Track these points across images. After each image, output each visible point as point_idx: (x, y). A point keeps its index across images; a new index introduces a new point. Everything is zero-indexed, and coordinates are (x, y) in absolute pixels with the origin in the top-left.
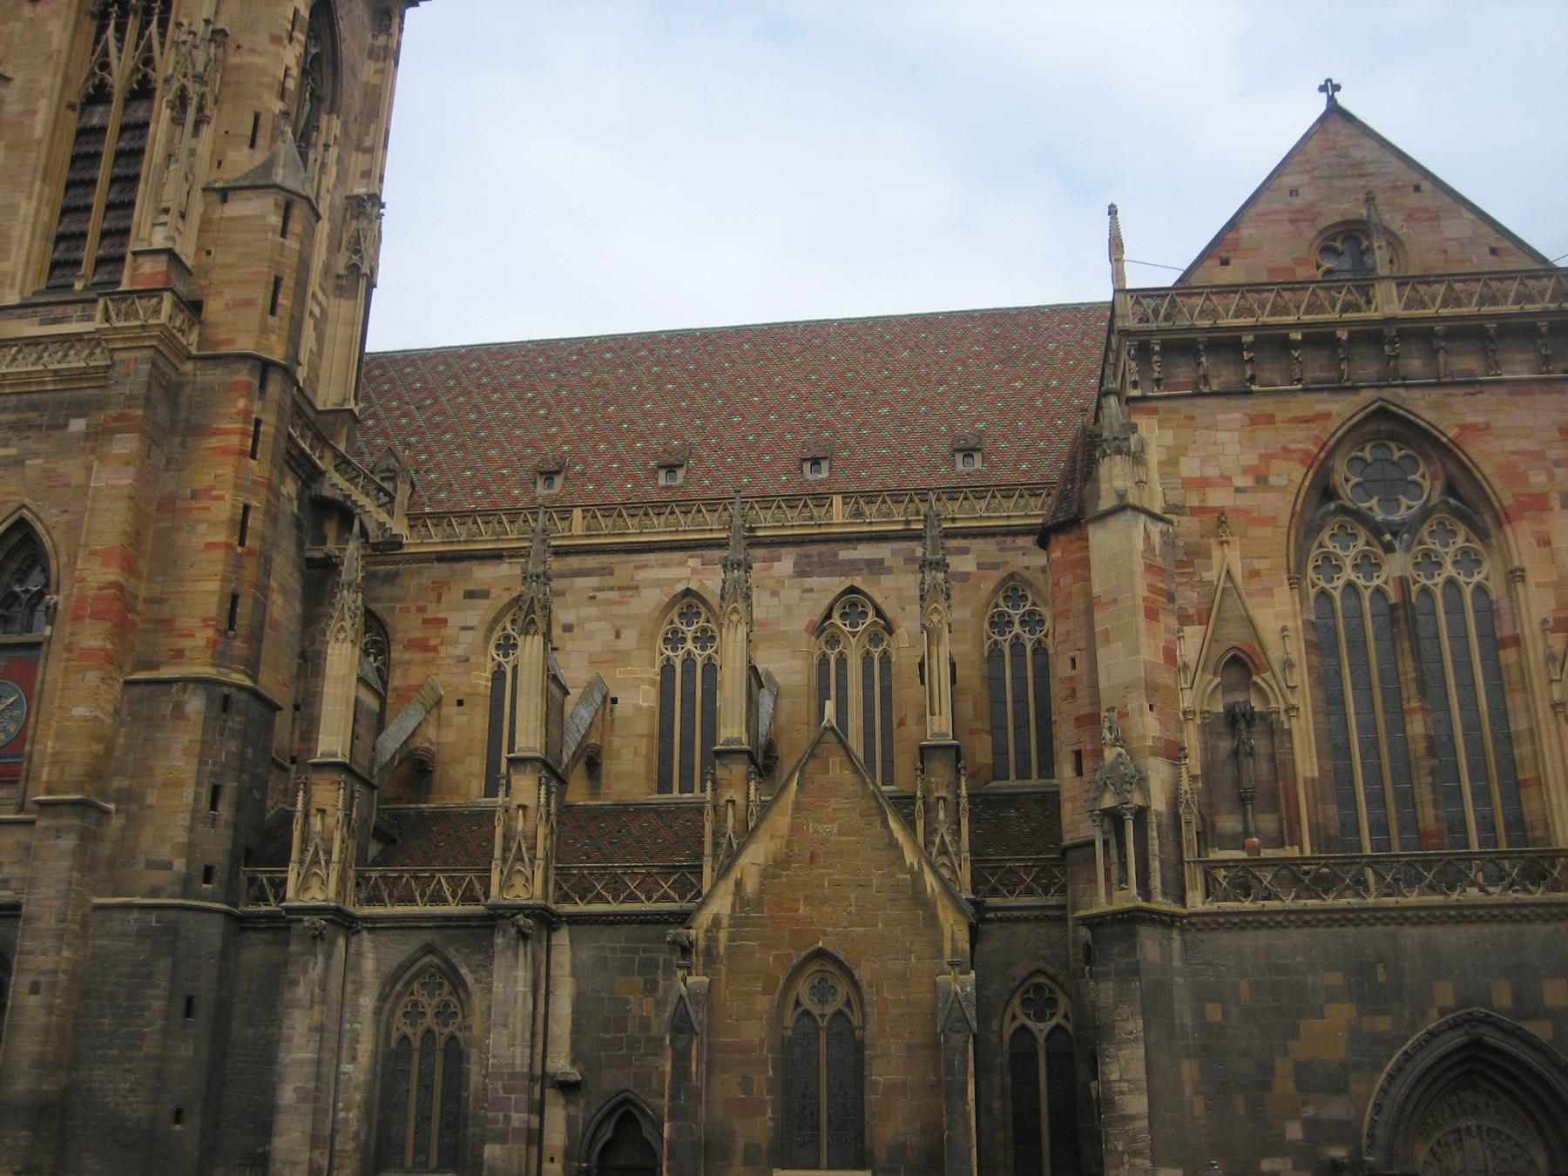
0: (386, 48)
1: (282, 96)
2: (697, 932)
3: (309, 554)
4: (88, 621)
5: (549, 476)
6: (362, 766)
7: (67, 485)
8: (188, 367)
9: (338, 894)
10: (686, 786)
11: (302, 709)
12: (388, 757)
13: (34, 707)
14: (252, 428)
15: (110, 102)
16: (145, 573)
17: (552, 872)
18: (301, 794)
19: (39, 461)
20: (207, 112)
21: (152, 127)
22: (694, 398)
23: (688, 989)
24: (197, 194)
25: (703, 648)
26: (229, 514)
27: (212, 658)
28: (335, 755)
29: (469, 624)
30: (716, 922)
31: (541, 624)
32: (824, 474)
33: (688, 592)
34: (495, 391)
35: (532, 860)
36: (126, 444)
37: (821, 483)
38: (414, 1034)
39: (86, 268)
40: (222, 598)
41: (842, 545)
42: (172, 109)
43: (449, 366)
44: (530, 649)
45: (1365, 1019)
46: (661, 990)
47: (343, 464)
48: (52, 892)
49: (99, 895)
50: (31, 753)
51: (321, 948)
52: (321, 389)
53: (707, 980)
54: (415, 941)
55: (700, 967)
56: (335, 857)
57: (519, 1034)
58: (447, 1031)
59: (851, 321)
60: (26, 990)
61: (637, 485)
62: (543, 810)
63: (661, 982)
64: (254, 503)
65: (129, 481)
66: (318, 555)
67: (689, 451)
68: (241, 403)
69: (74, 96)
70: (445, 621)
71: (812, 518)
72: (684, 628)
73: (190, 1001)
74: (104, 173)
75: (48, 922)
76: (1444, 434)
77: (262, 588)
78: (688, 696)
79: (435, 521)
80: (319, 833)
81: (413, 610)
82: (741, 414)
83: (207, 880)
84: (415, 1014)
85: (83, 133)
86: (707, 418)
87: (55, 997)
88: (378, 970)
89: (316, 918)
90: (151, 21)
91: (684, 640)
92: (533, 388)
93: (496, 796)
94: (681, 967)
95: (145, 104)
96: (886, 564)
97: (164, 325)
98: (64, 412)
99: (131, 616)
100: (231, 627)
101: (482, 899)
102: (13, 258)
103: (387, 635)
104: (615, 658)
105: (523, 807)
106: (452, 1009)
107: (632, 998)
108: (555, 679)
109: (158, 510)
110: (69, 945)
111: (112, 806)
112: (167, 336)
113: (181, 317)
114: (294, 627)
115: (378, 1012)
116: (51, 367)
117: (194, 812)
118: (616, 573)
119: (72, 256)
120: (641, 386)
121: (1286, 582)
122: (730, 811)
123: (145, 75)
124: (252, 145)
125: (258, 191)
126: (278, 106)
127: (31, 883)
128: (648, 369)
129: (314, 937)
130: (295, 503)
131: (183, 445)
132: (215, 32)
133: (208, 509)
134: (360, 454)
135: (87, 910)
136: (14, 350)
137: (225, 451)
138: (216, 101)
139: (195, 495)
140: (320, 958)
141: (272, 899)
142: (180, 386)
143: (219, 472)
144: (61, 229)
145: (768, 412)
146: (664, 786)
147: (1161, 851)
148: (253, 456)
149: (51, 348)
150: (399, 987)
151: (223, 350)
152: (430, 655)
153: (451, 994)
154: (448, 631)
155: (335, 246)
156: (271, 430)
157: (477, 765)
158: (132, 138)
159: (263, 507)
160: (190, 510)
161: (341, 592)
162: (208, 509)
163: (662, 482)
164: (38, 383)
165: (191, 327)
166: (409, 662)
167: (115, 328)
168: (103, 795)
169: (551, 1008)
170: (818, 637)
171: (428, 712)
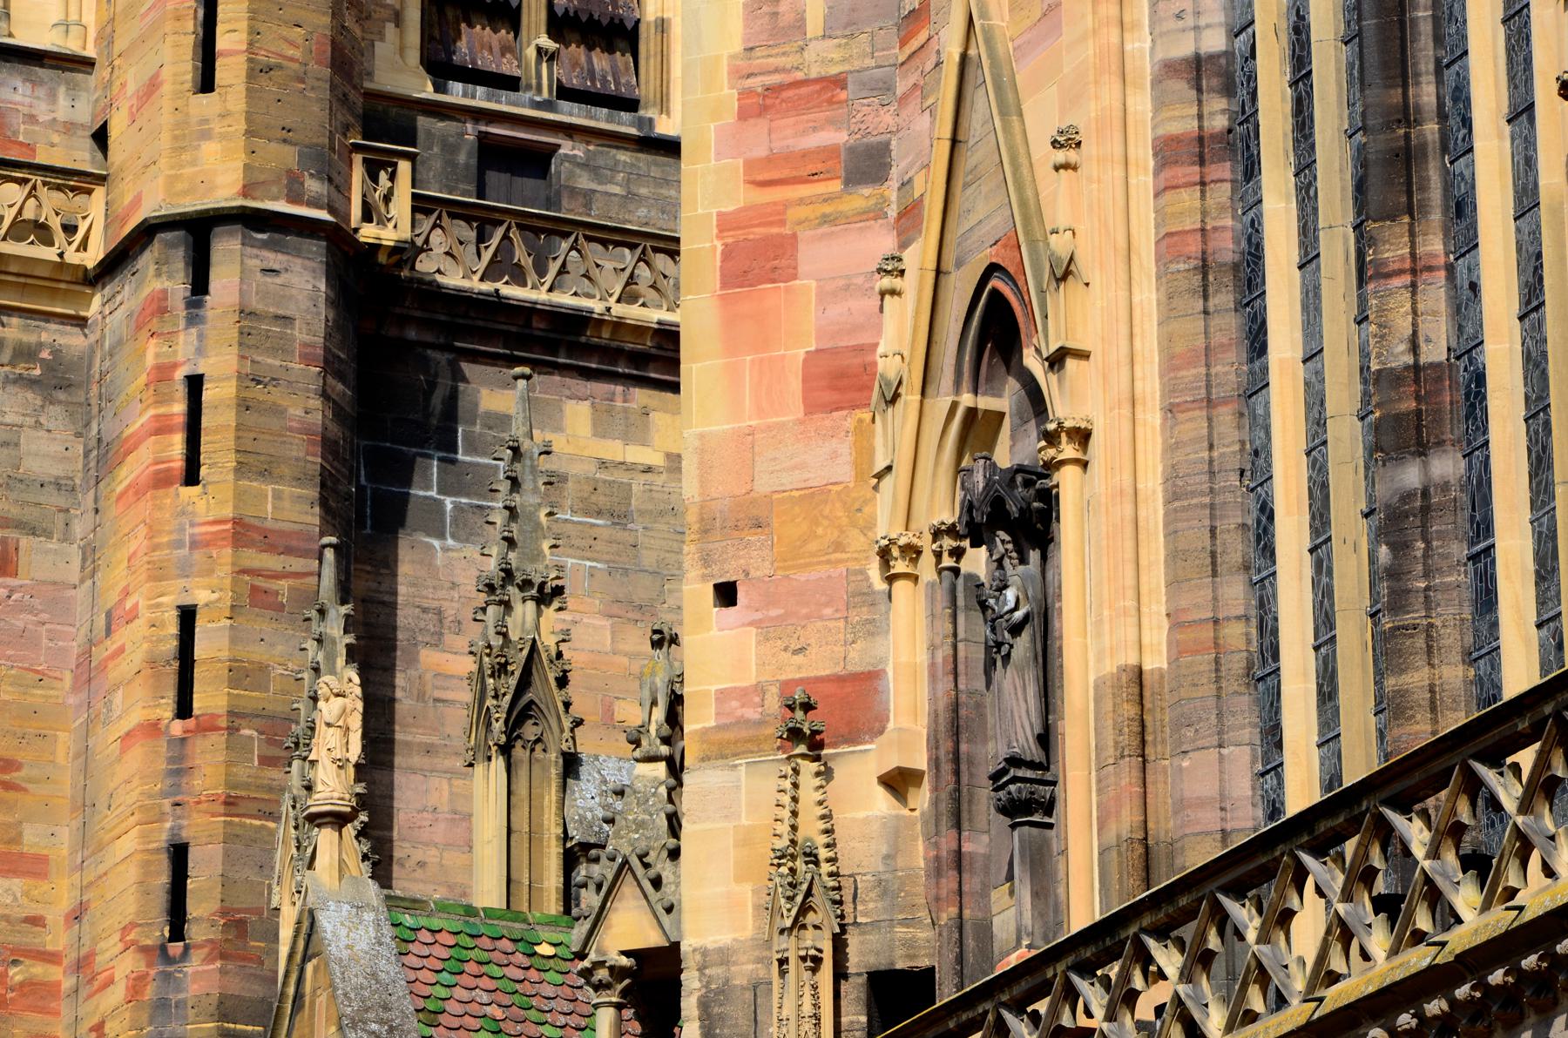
14: (179, 408)
64: (201, 596)
99: (16, 974)
100: (177, 933)
137: (137, 491)
148: (191, 476)
162: (121, 650)
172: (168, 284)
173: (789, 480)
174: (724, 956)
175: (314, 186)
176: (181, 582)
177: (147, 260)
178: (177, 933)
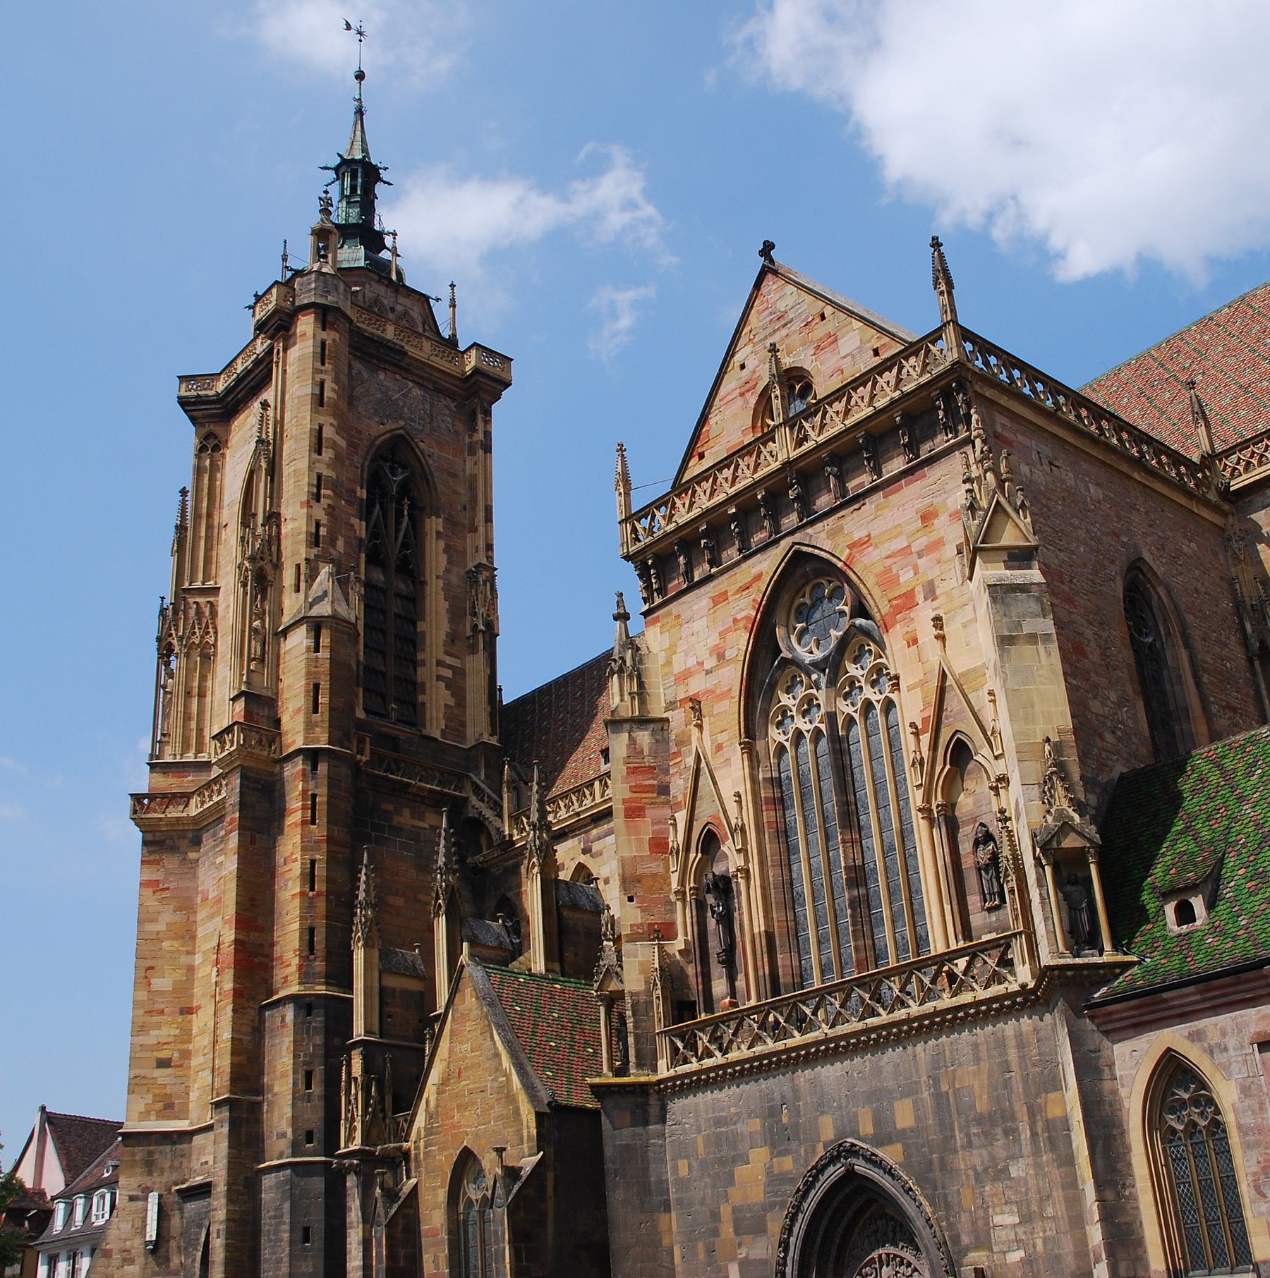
40: (301, 933)
45: (775, 1160)
64: (318, 857)
76: (840, 560)
99: (256, 960)
100: (311, 949)
117: (294, 1093)
121: (739, 748)
124: (298, 591)
147: (635, 1027)
148: (313, 822)
151: (291, 750)
156: (325, 799)
173: (648, 871)
174: (637, 994)
175: (346, 743)
177: (299, 759)
178: (311, 949)
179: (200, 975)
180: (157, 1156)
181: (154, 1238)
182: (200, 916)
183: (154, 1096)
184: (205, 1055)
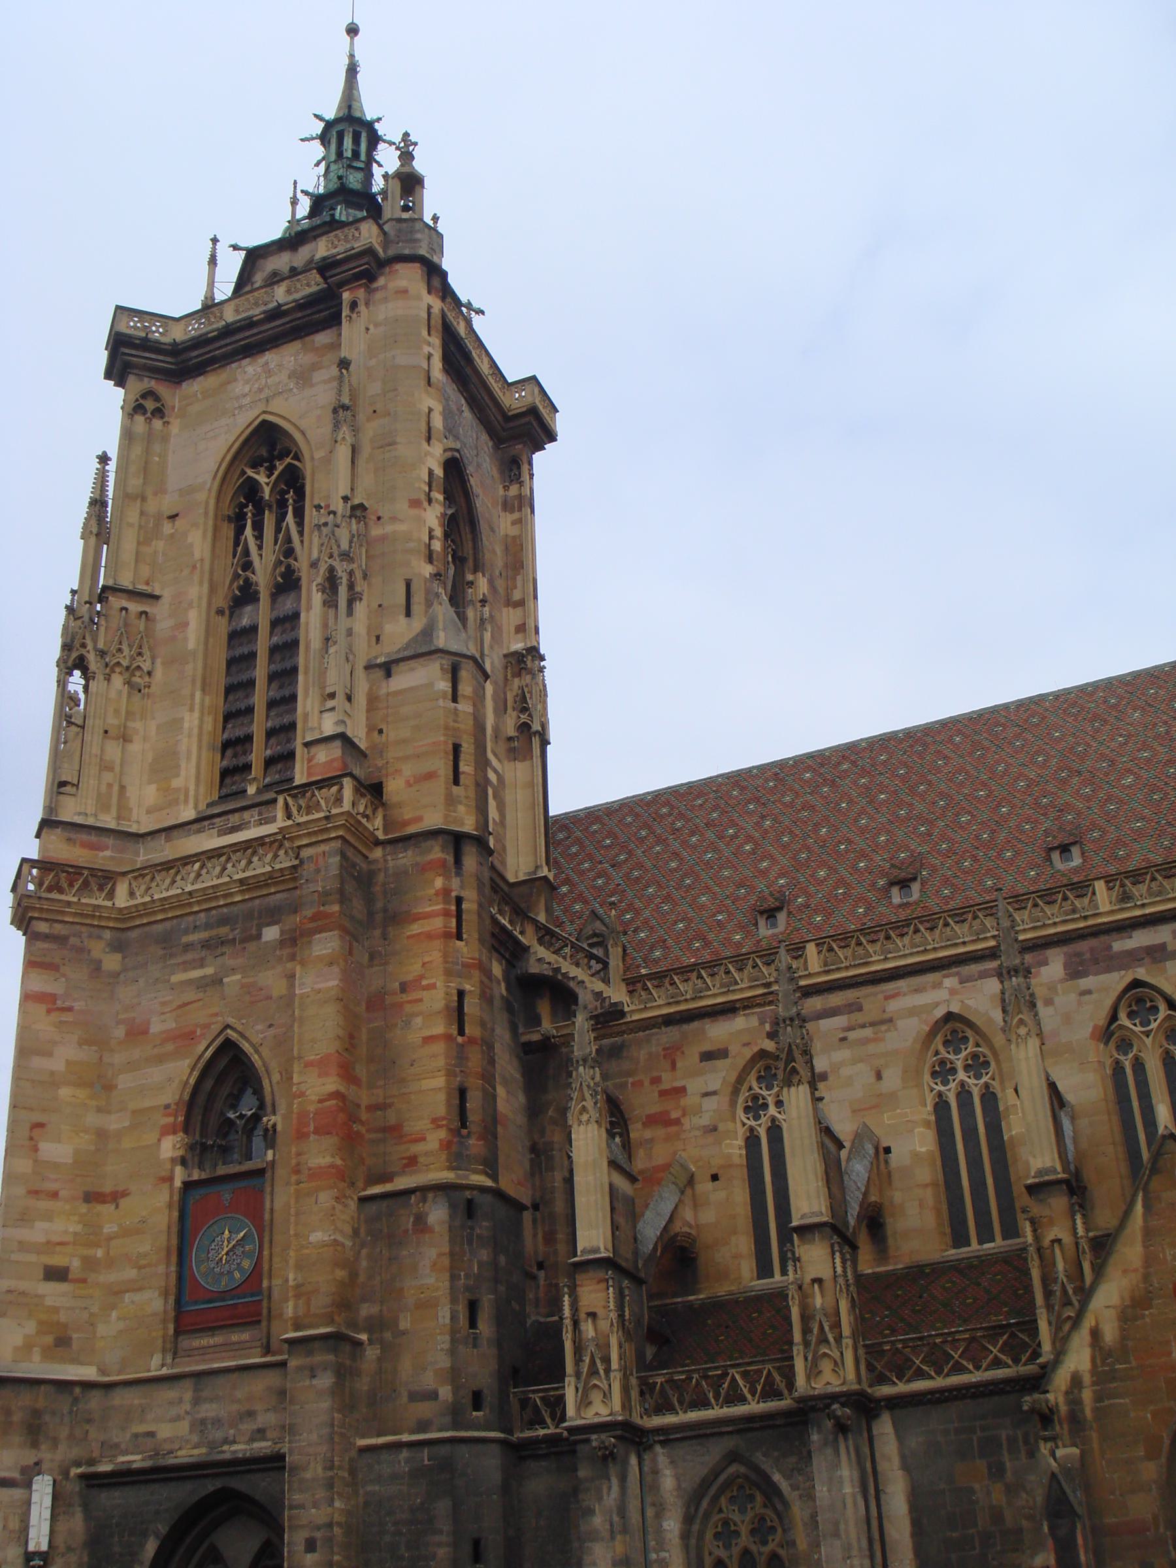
0: (520, 497)
1: (430, 559)
2: (1056, 1394)
3: (524, 1039)
4: (312, 1137)
5: (770, 914)
6: (627, 1260)
7: (269, 998)
8: (378, 853)
9: (623, 1407)
10: (986, 1235)
11: (541, 1207)
12: (651, 1247)
13: (266, 1239)
14: (453, 908)
15: (258, 600)
16: (364, 1079)
17: (861, 1351)
18: (566, 1298)
19: (238, 977)
20: (358, 589)
21: (303, 615)
22: (911, 805)
23: (1059, 1464)
24: (360, 673)
25: (978, 1076)
26: (444, 1002)
27: (448, 1160)
28: (597, 1250)
29: (711, 1089)
30: (1076, 1381)
31: (804, 1073)
32: (1077, 861)
33: (949, 1017)
34: (693, 834)
35: (839, 1338)
36: (326, 944)
37: (1076, 870)
38: (731, 1557)
39: (257, 770)
40: (449, 1094)
41: (1114, 935)
42: (323, 592)
43: (637, 815)
44: (798, 1098)
46: (1009, 1474)
47: (547, 936)
48: (314, 1437)
49: (363, 1437)
50: (270, 1288)
51: (613, 1471)
52: (510, 860)
53: (1075, 1451)
54: (715, 1451)
55: (1066, 1437)
56: (615, 1365)
57: (855, 1544)
58: (766, 1549)
59: (1067, 692)
60: (302, 1548)
61: (869, 908)
62: (841, 1280)
63: (1008, 1465)
64: (468, 987)
65: (335, 983)
66: (535, 1037)
67: (918, 860)
68: (439, 883)
69: (221, 601)
70: (682, 1090)
71: (1074, 911)
72: (952, 1057)
73: (476, 1543)
74: (261, 671)
75: (315, 1471)
77: (488, 1078)
78: (970, 1133)
79: (656, 983)
80: (593, 1339)
81: (647, 1083)
82: (969, 813)
83: (477, 1406)
84: (727, 1533)
85: (236, 636)
86: (931, 823)
87: (333, 1553)
88: (679, 1488)
89: (603, 1436)
90: (286, 513)
91: (953, 1071)
92: (733, 823)
93: (772, 1276)
94: (1046, 1439)
95: (293, 595)
96: (1169, 948)
97: (348, 812)
98: (255, 922)
99: (356, 1127)
100: (464, 1125)
101: (786, 1392)
102: (183, 773)
103: (621, 1113)
104: (882, 1102)
105: (818, 1281)
106: (769, 1524)
107: (977, 1486)
108: (827, 1131)
109: (368, 1009)
110: (340, 1495)
111: (364, 1337)
112: (353, 824)
113: (363, 801)
114: (521, 1119)
115: (685, 1536)
116: (236, 877)
117: (453, 1332)
118: (866, 1007)
119: (242, 761)
120: (851, 802)
122: (1058, 1252)
123: (289, 567)
124: (408, 614)
125: (421, 660)
126: (428, 570)
127: (290, 1429)
128: (855, 783)
129: (605, 1458)
130: (503, 985)
131: (385, 937)
132: (353, 508)
133: (421, 1000)
134: (560, 925)
135: (354, 1454)
136: (197, 865)
137: (429, 936)
138: (365, 577)
139: (404, 987)
140: (615, 1481)
141: (549, 1421)
142: (372, 874)
143: (427, 959)
144: (226, 736)
145: (999, 805)
146: (959, 1238)
148: (459, 937)
149: (234, 858)
150: (705, 1504)
151: (412, 829)
152: (673, 1129)
153: (765, 1506)
154: (690, 1100)
155: (501, 708)
156: (475, 907)
157: (744, 1244)
158: (283, 632)
159: (478, 991)
160: (400, 1005)
161: (577, 1069)
162: (421, 1000)
163: (896, 899)
164: (225, 896)
165: (374, 811)
166: (652, 1140)
167: (298, 824)
168: (353, 1325)
169: (884, 1508)
170: (1106, 1043)
171: (682, 1192)
172: (447, 857)
176: (459, 979)
179: (127, 1143)
180: (47, 1418)
181: (44, 1547)
182: (118, 1058)
183: (41, 1323)
184: (144, 1267)
